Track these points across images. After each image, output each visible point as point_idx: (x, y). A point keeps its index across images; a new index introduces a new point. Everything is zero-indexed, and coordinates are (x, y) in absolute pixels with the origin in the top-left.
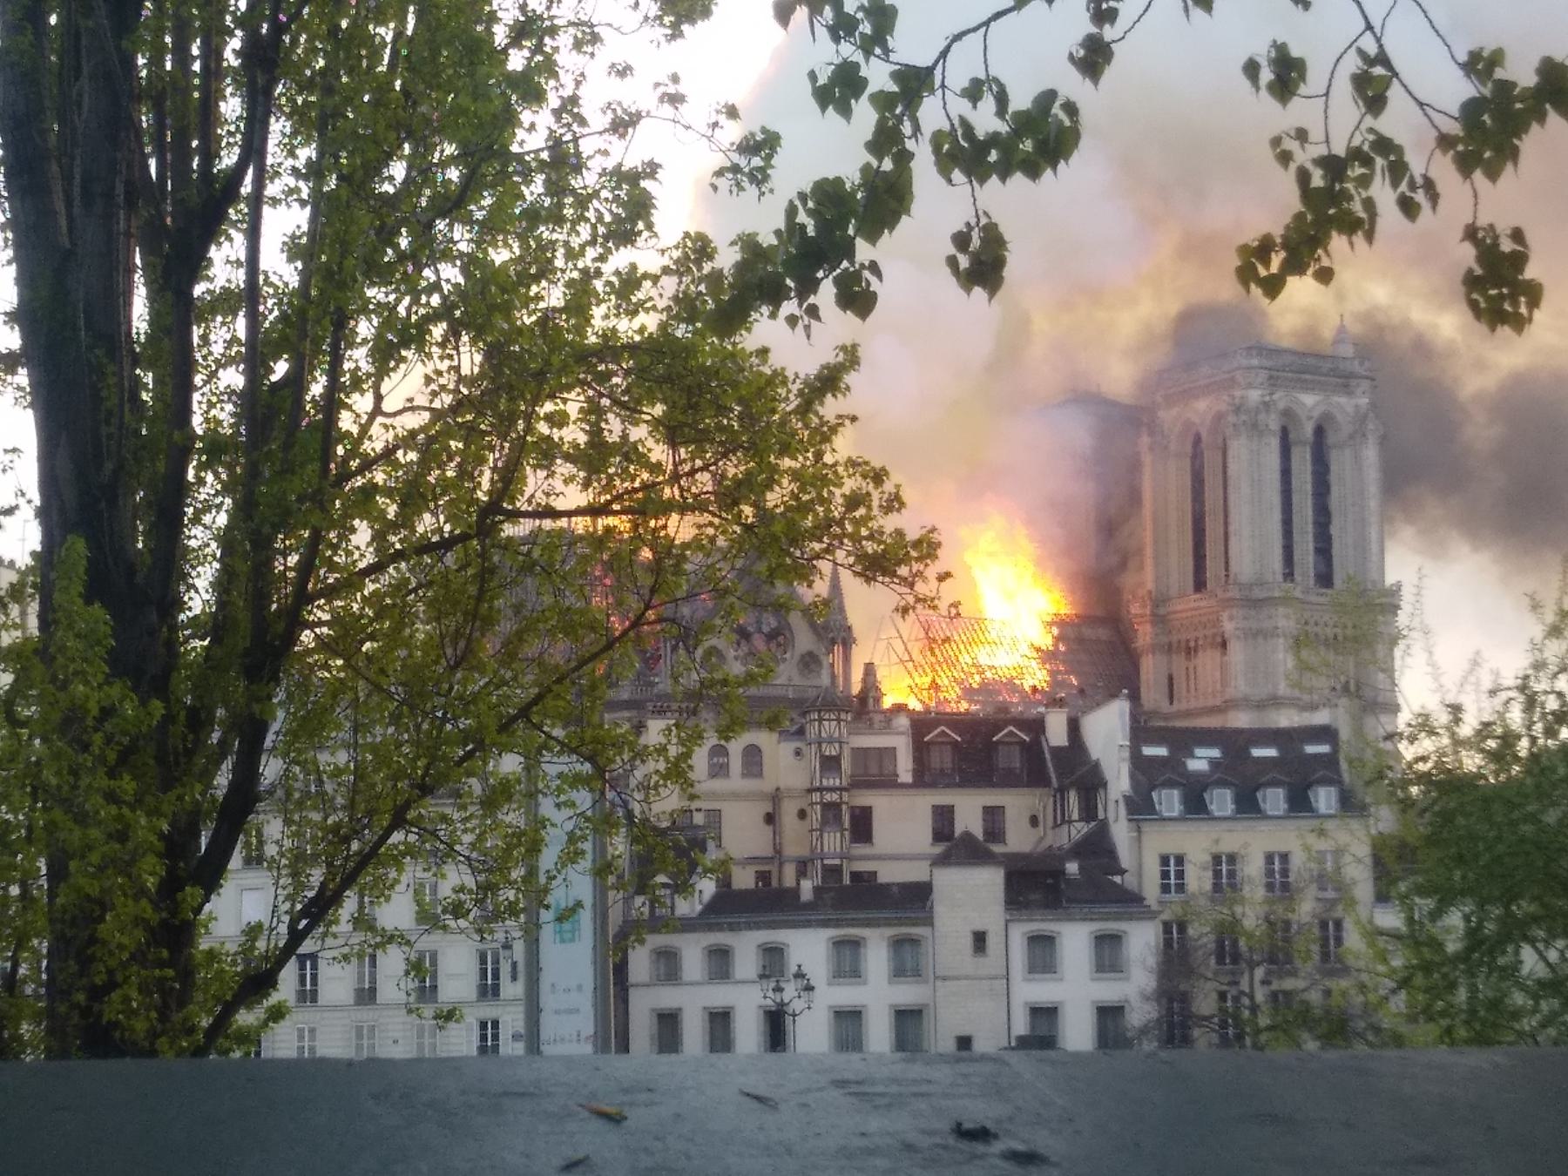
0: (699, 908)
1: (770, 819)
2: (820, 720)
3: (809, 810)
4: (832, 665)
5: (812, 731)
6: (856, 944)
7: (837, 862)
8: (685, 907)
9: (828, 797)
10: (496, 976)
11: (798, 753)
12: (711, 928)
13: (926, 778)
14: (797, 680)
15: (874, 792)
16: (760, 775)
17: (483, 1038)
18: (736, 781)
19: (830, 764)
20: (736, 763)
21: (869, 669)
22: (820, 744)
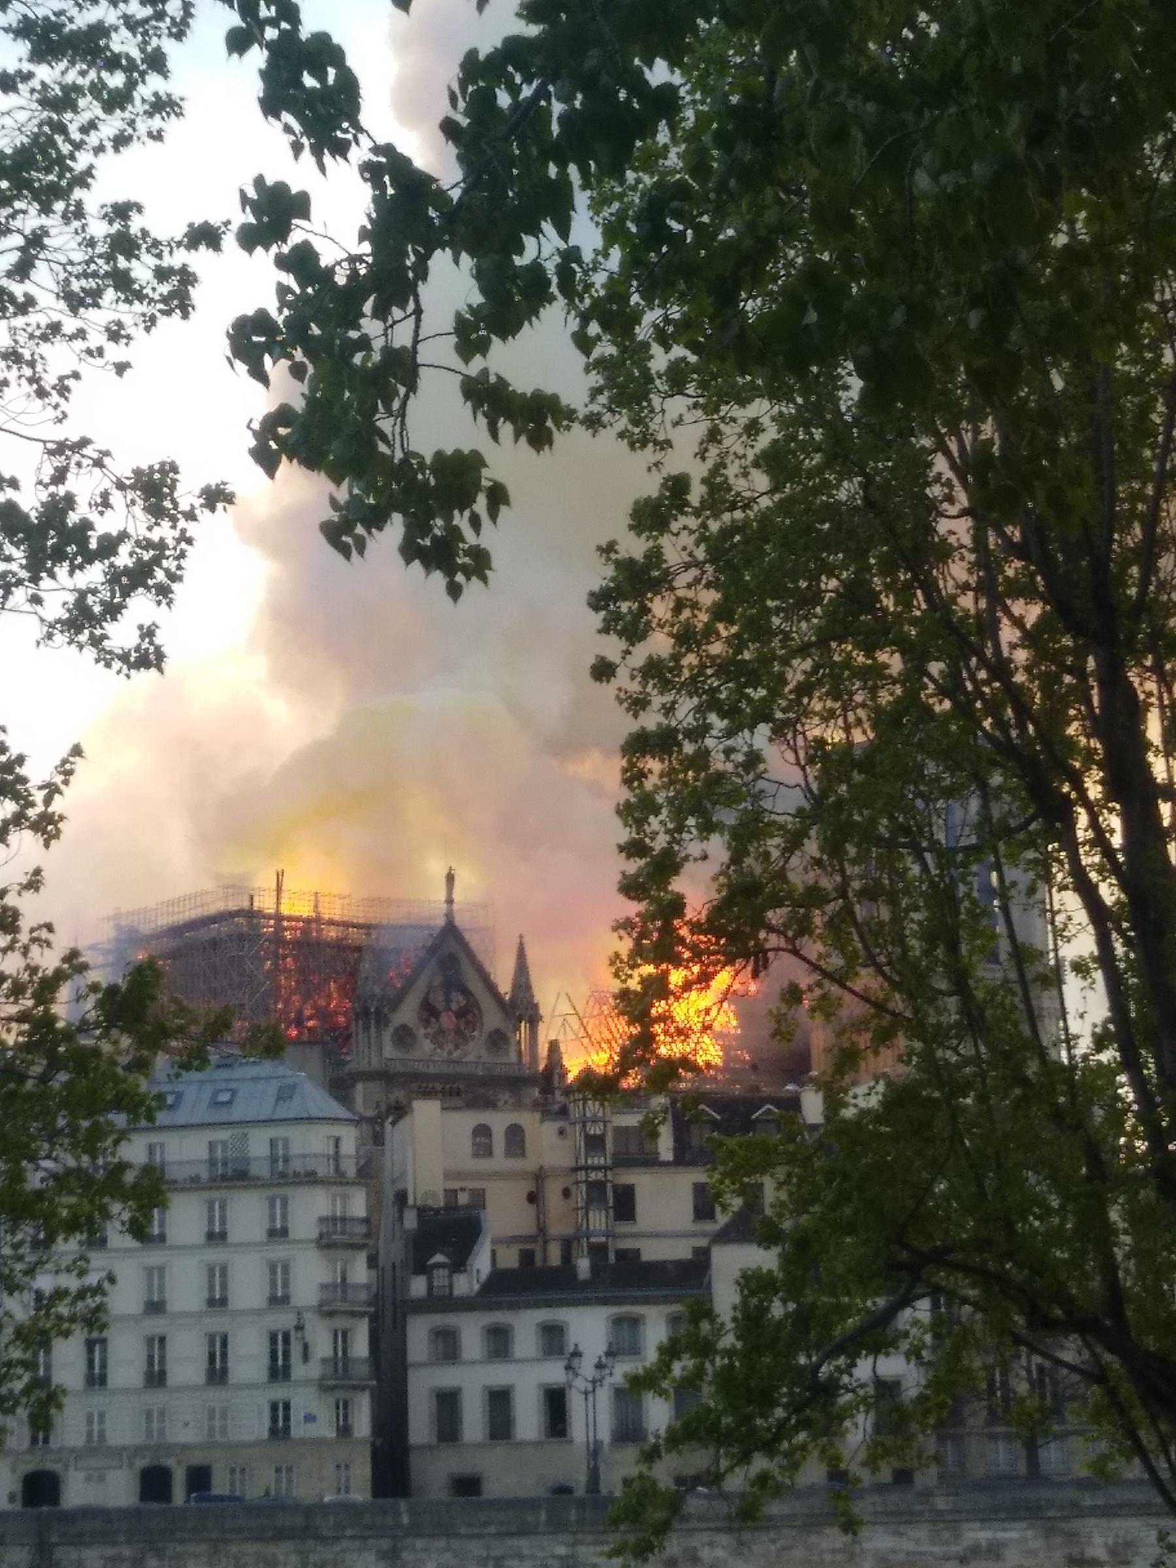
0: (476, 1287)
1: (532, 1198)
2: (585, 1100)
3: (573, 1189)
4: (519, 1042)
5: (575, 1112)
6: (635, 1322)
7: (603, 1239)
8: (464, 1285)
9: (593, 1176)
10: (286, 1355)
11: (561, 1132)
12: (490, 1307)
13: (688, 1156)
14: (486, 1057)
15: (636, 1170)
16: (523, 1154)
17: (274, 1419)
18: (499, 1161)
19: (595, 1143)
20: (499, 1142)
21: (554, 1046)
22: (584, 1124)
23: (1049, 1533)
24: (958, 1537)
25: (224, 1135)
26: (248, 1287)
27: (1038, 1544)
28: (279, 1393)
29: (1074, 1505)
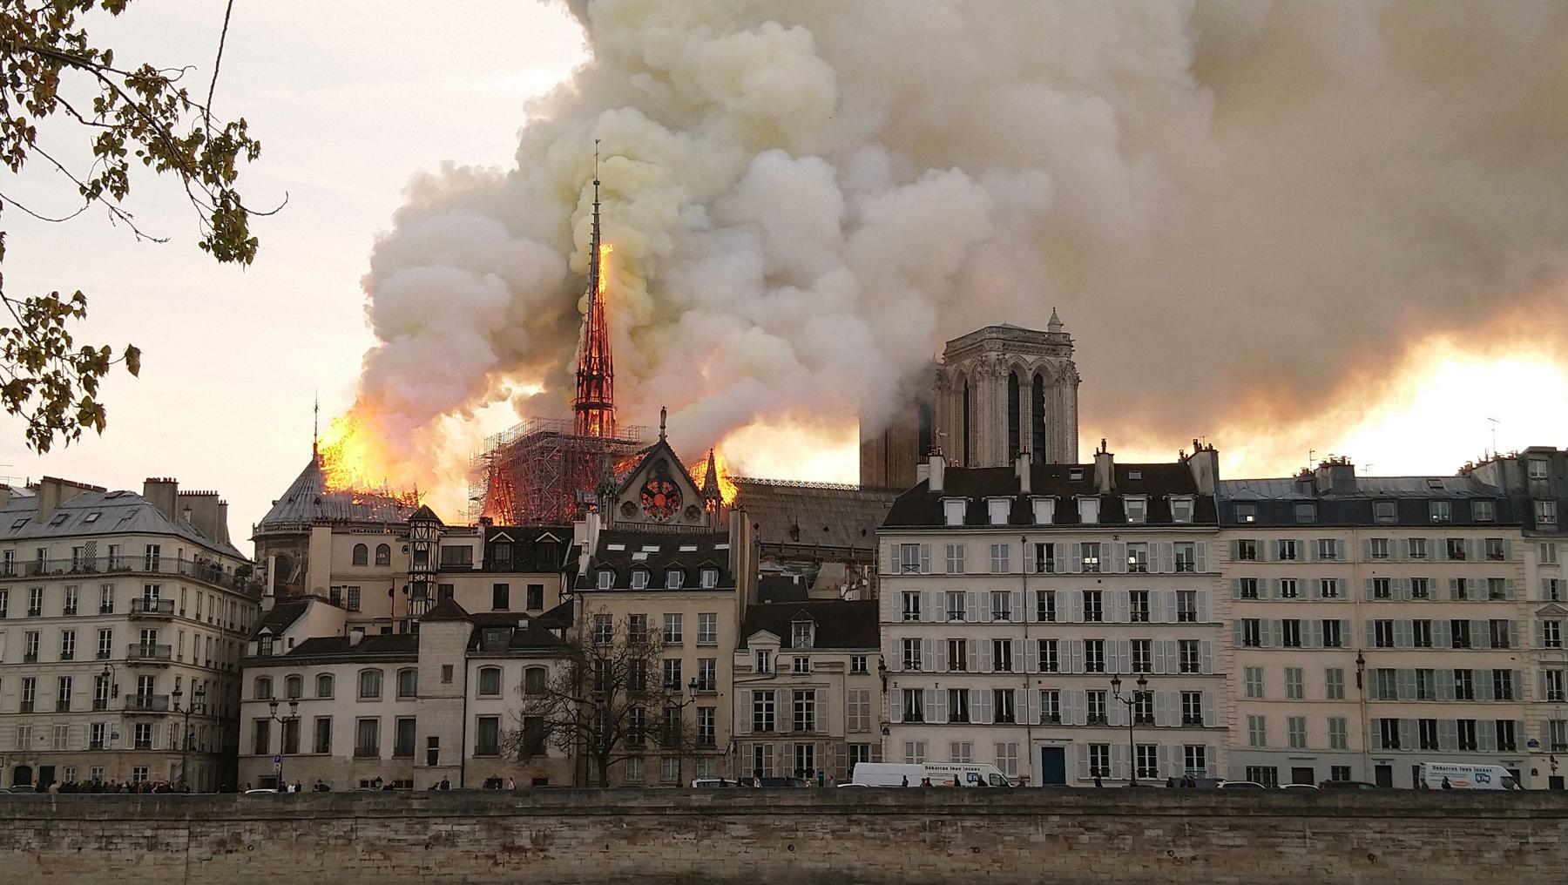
24: (426, 828)
25: (82, 543)
29: (511, 807)
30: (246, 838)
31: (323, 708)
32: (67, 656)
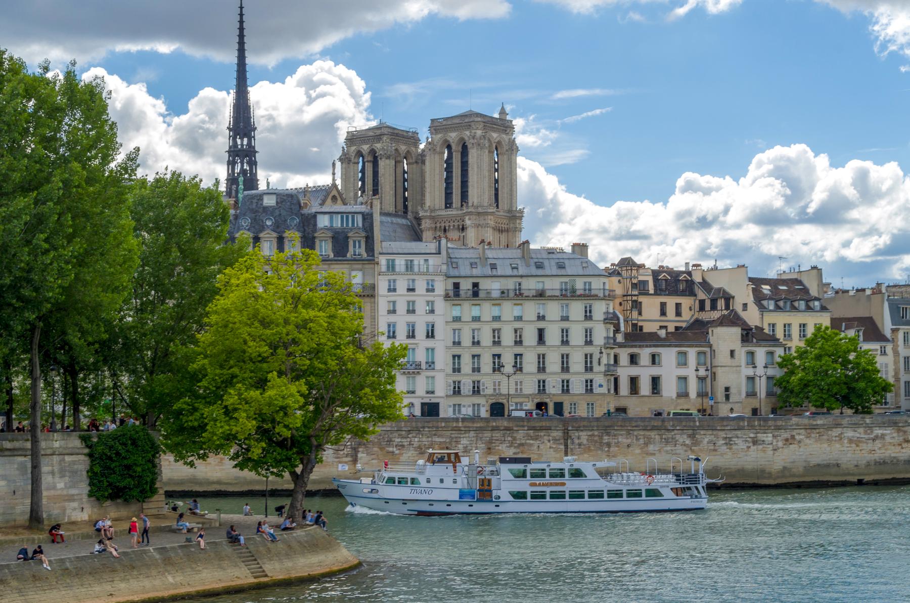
11: (619, 281)
23: (899, 431)
26: (577, 337)
27: (895, 435)
28: (589, 376)
30: (797, 437)
31: (655, 371)
32: (565, 342)
